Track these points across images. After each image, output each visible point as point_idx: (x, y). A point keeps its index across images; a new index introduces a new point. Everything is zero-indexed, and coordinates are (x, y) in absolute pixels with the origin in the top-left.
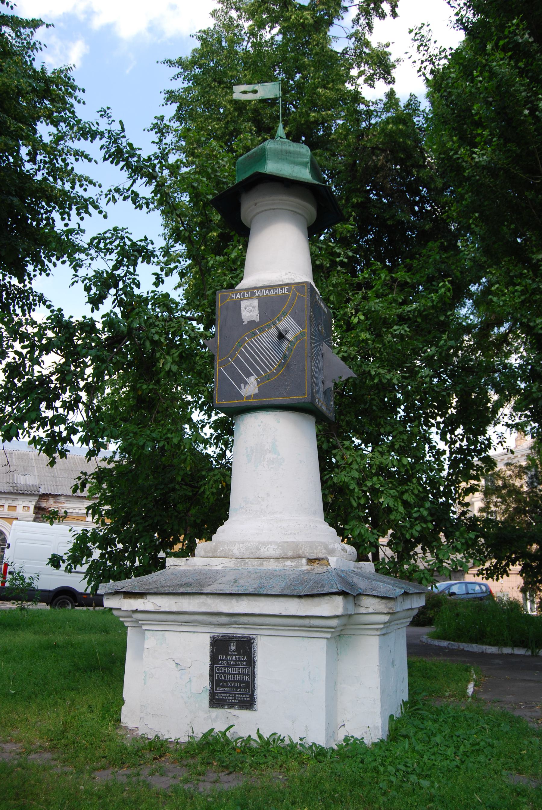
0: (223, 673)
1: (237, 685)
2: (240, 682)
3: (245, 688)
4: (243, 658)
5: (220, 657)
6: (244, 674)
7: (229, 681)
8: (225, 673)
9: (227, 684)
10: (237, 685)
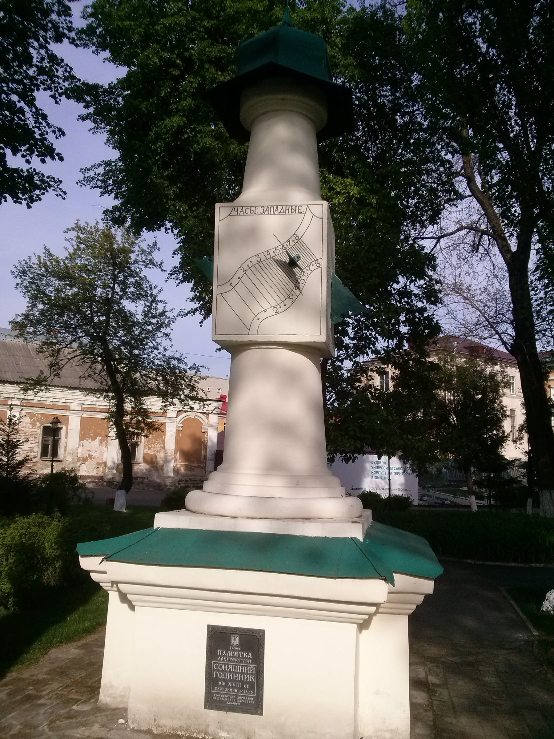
0: (222, 671)
1: (239, 685)
2: (243, 683)
3: (248, 690)
4: (248, 655)
5: (219, 652)
6: (247, 674)
7: (230, 680)
8: (225, 671)
9: (227, 684)
10: (239, 685)
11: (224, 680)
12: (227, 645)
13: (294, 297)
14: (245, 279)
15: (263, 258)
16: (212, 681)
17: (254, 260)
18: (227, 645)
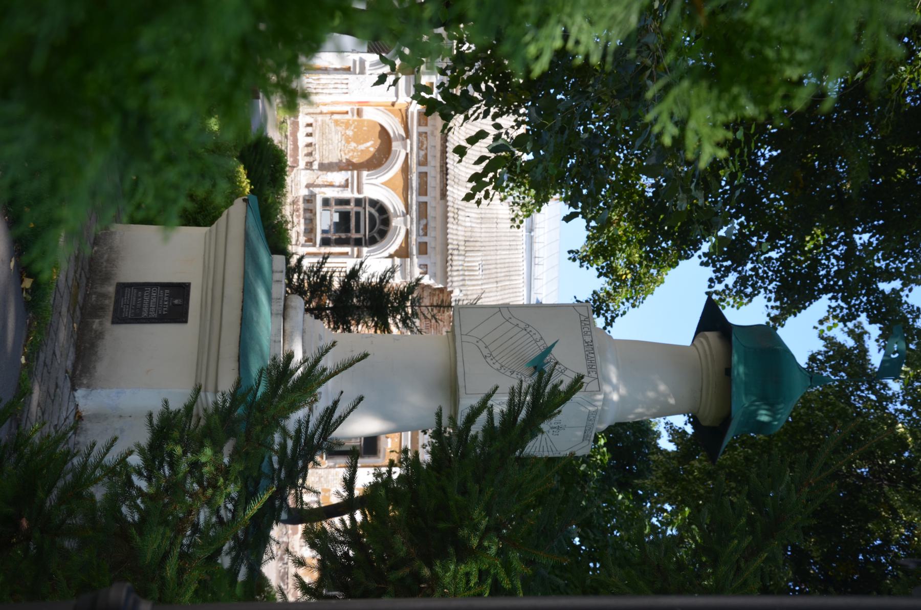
1: (139, 306)
10: (139, 306)
11: (143, 296)
13: (502, 371)
14: (517, 329)
15: (539, 344)
16: (142, 287)
17: (537, 337)
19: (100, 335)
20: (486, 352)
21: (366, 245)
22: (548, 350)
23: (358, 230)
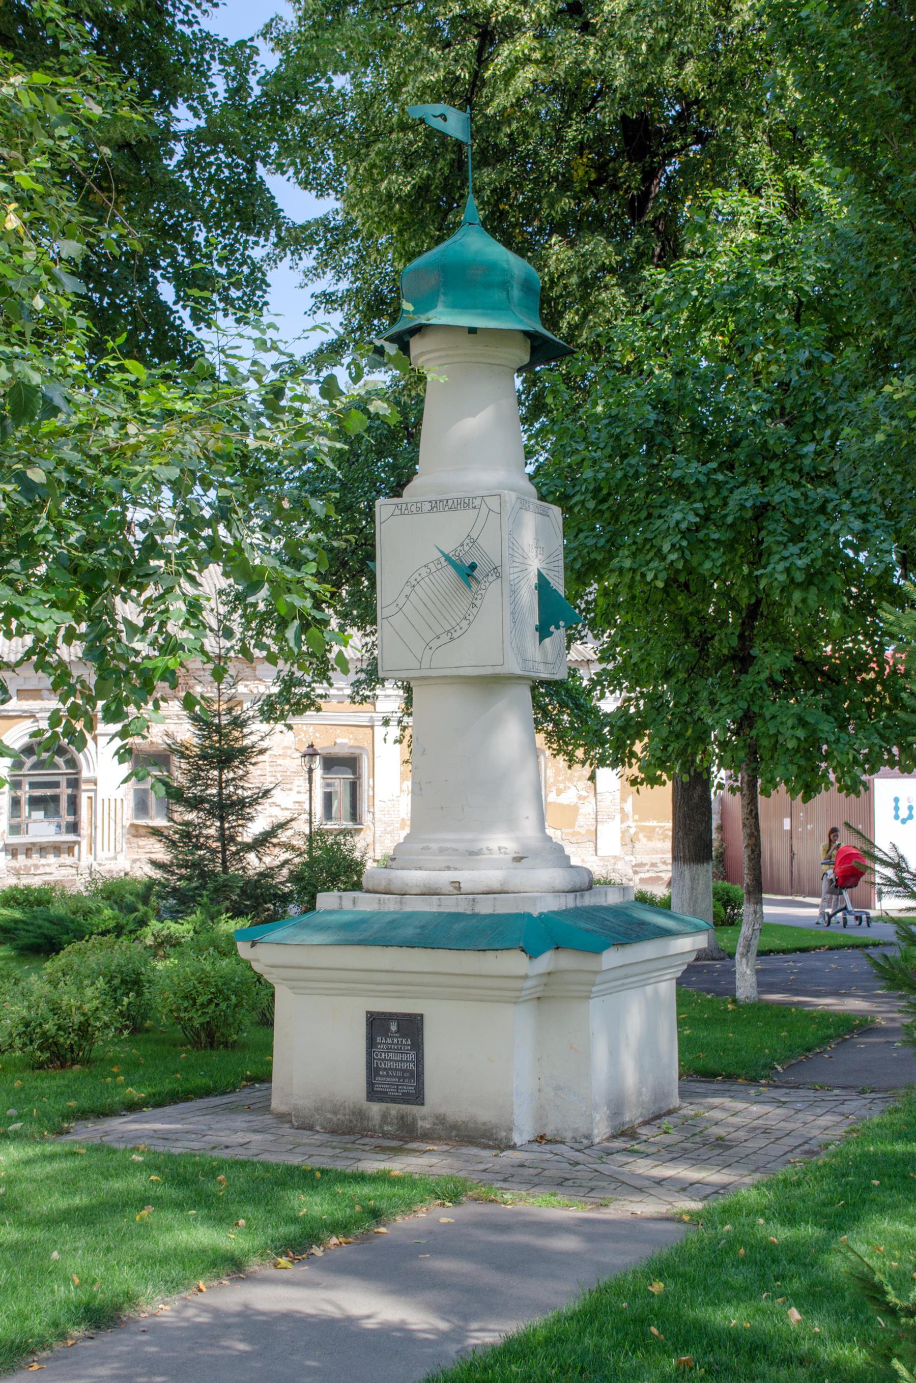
2: (404, 1071)
10: (399, 1074)
12: (386, 1033)
14: (413, 597)
16: (372, 1071)
17: (424, 571)
18: (386, 1033)
19: (440, 1120)
20: (445, 638)
21: (78, 773)
22: (447, 558)
23: (56, 785)
